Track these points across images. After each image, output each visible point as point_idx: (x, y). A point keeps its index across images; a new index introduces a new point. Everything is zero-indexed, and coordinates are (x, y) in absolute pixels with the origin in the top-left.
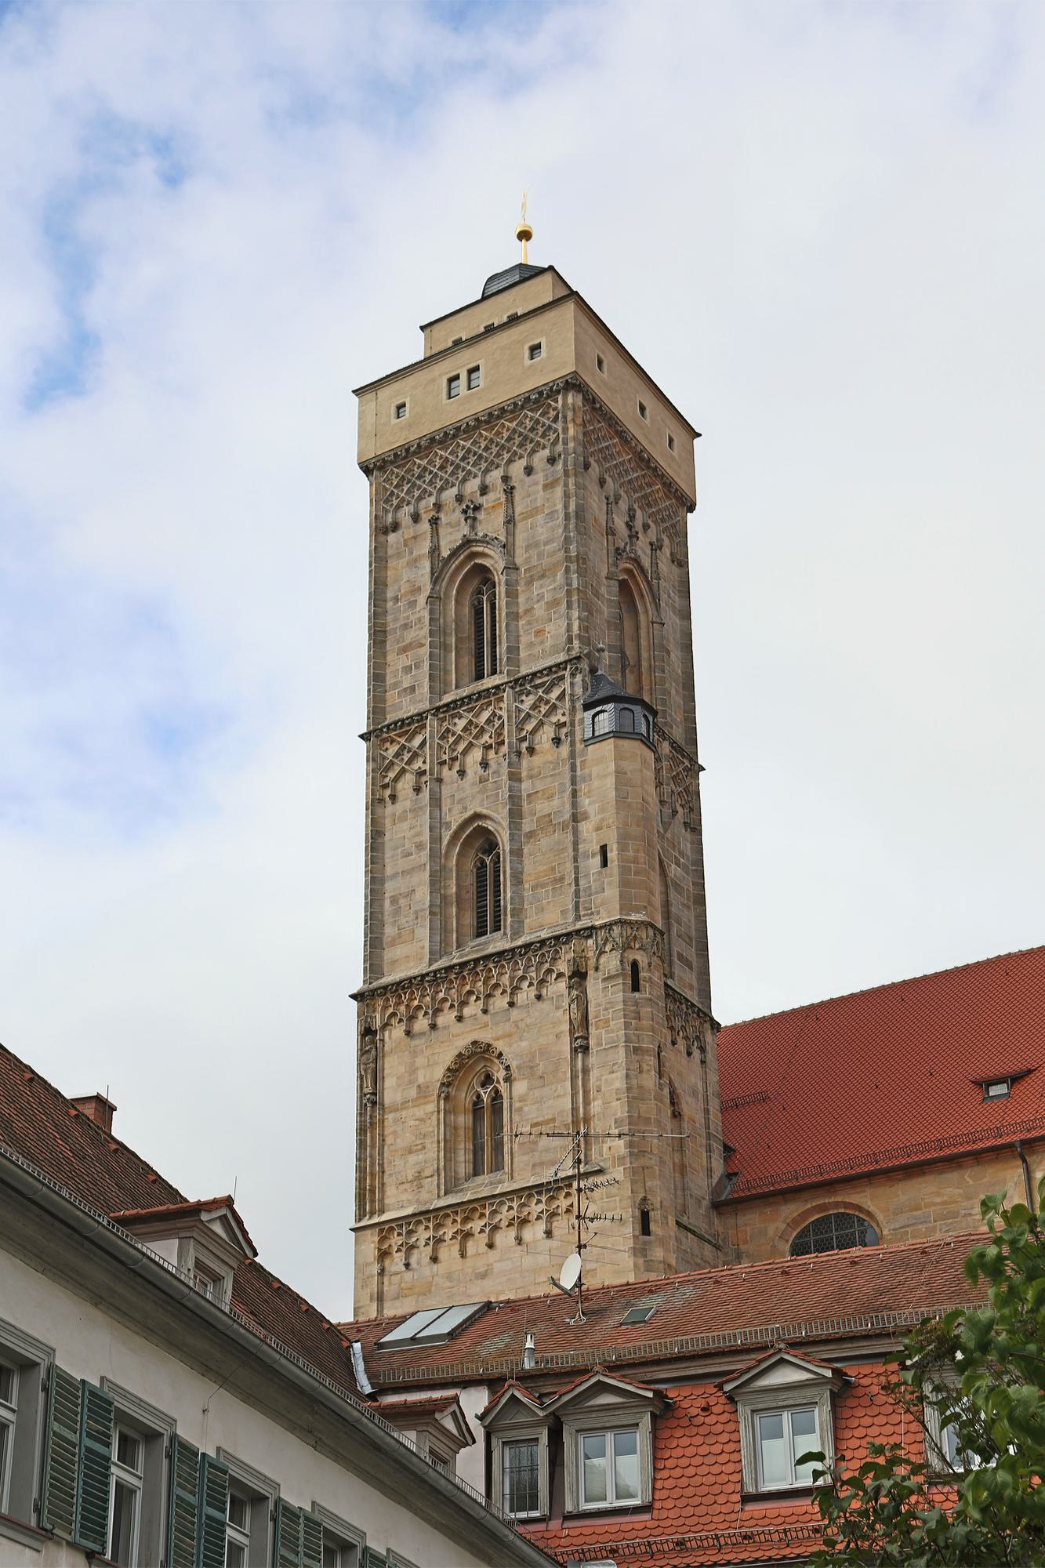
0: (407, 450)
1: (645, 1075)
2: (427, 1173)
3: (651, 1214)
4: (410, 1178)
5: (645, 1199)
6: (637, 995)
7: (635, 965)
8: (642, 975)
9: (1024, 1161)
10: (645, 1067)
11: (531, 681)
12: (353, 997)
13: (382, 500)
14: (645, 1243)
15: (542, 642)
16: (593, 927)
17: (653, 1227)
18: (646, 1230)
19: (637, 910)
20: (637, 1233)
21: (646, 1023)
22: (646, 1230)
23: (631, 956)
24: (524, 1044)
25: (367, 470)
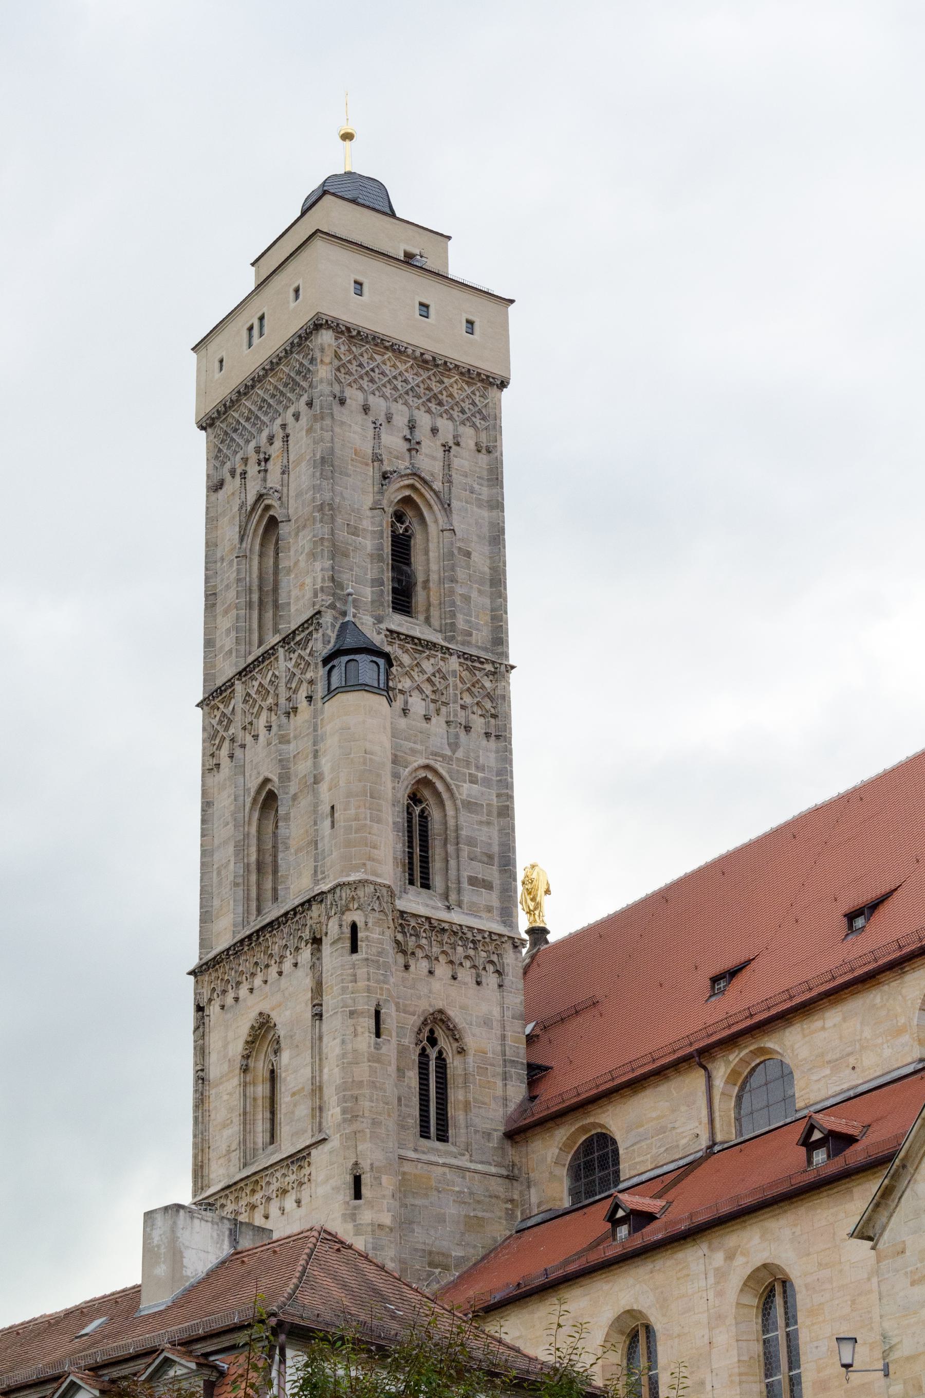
0: (225, 405)
1: (359, 1038)
2: (233, 1148)
3: (363, 1177)
4: (224, 1152)
5: (356, 1164)
6: (355, 956)
7: (354, 927)
8: (360, 935)
9: (705, 1068)
10: (360, 1030)
11: (293, 639)
12: (190, 973)
13: (217, 456)
14: (355, 1208)
15: (303, 596)
16: (323, 893)
17: (364, 1191)
18: (358, 1195)
19: (355, 868)
20: (348, 1199)
21: (361, 984)
22: (358, 1195)
23: (349, 917)
24: (288, 1013)
25: (202, 428)
